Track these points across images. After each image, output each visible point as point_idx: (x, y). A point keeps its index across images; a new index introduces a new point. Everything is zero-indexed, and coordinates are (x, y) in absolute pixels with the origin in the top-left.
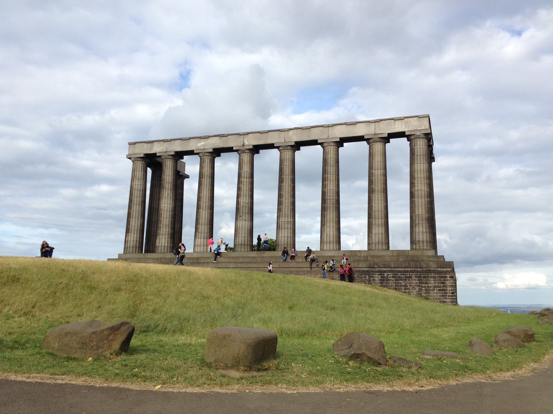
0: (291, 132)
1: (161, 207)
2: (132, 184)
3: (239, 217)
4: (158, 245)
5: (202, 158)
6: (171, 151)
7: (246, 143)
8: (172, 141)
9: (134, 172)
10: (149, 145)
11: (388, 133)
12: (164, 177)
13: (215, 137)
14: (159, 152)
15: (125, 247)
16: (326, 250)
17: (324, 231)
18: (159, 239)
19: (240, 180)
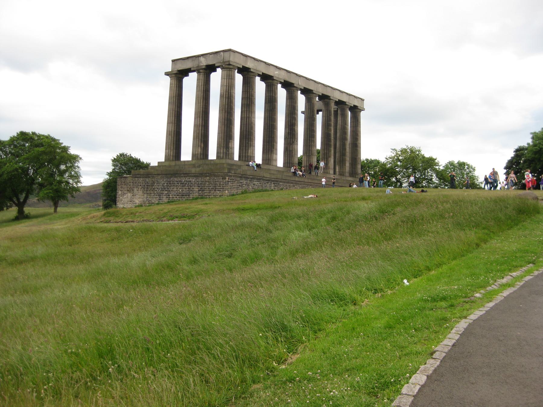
0: (320, 85)
1: (252, 121)
2: (232, 91)
3: (295, 141)
4: (251, 155)
5: (275, 85)
6: (259, 71)
7: (300, 84)
8: (260, 62)
9: (232, 80)
10: (245, 57)
11: (354, 105)
12: (253, 93)
13: (284, 71)
14: (253, 69)
15: (229, 153)
16: (331, 174)
17: (330, 160)
18: (251, 150)
19: (295, 111)
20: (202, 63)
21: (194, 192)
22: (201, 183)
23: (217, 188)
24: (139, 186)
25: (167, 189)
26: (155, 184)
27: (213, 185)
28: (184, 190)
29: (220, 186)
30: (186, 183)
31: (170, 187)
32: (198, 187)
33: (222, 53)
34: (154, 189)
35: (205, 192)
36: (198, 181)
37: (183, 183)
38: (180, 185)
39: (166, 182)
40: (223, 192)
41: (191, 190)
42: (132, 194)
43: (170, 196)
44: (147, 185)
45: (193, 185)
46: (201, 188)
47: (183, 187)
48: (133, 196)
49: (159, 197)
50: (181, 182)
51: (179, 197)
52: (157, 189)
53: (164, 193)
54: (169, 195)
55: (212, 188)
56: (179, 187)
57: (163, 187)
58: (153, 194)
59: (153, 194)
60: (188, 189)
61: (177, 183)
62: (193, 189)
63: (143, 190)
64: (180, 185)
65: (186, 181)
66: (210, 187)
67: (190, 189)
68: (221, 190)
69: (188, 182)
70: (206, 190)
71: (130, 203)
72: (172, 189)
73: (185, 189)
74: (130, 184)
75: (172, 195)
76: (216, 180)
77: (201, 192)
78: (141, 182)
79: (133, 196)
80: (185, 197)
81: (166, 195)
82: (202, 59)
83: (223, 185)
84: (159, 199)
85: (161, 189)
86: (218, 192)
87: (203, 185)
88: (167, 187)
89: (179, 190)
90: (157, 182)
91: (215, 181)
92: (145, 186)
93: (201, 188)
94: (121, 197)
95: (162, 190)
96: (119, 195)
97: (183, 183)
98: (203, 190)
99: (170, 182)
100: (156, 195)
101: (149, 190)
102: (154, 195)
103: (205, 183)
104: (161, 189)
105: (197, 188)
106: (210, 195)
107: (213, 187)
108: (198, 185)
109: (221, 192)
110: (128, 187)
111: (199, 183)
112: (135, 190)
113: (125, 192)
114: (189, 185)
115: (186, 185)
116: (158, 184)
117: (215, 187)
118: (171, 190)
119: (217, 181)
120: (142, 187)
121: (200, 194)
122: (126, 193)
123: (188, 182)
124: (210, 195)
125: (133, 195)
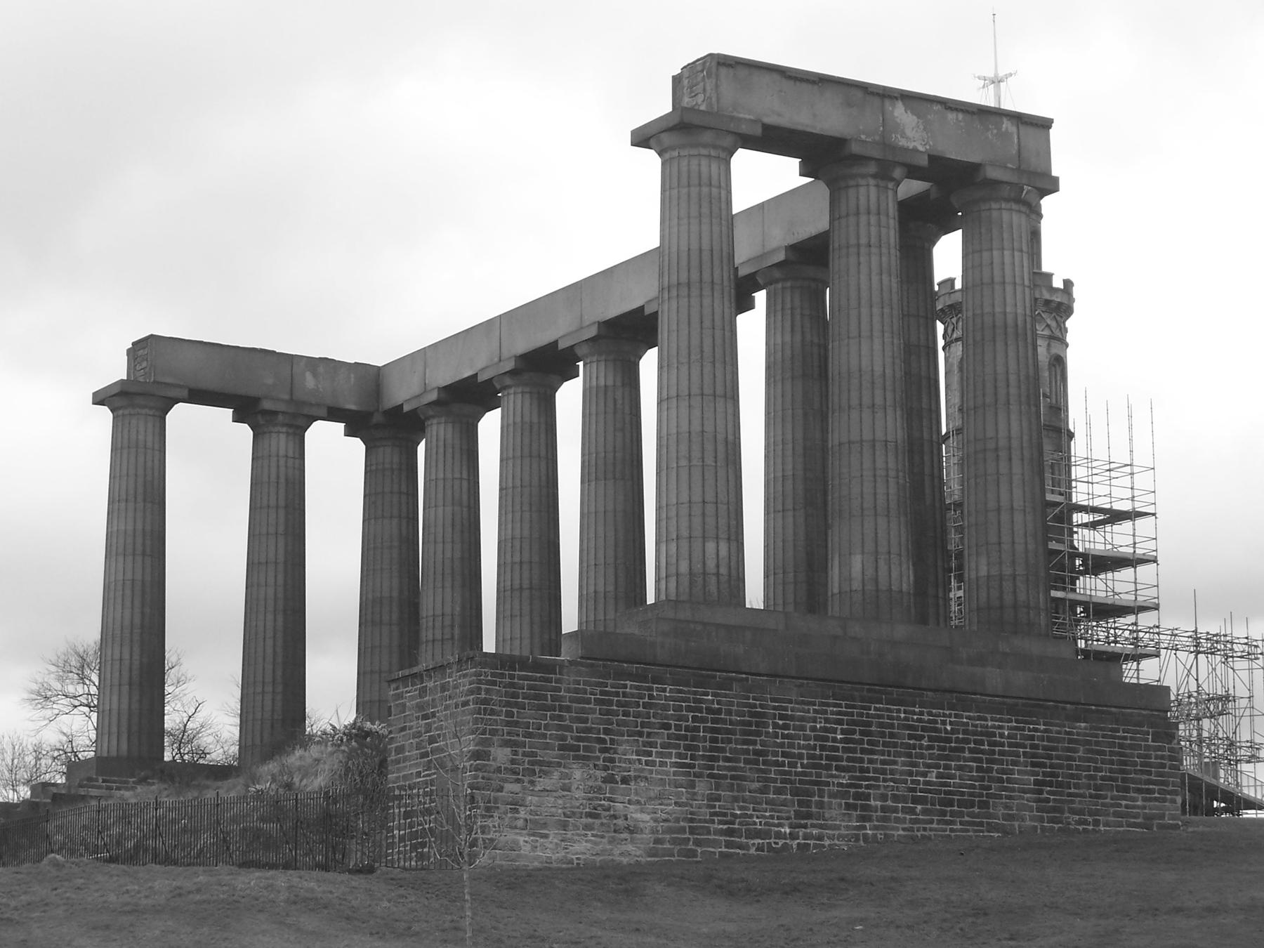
20: (903, 135)
21: (1013, 790)
22: (1045, 748)
23: (1134, 781)
24: (649, 725)
25: (849, 759)
26: (766, 725)
27: (1112, 762)
28: (953, 777)
29: (1150, 773)
30: (967, 741)
31: (863, 751)
32: (1034, 765)
33: (1007, 125)
34: (756, 753)
35: (1070, 795)
36: (1032, 738)
37: (949, 740)
38: (930, 748)
39: (840, 722)
40: (1164, 800)
41: (991, 779)
42: (600, 774)
43: (872, 803)
44: (713, 730)
45: (1002, 753)
46: (1052, 775)
47: (947, 758)
48: (605, 781)
49: (800, 803)
50: (936, 730)
51: (924, 812)
52: (784, 755)
53: (828, 784)
54: (867, 797)
55: (1111, 779)
56: (922, 756)
57: (823, 748)
58: (756, 785)
59: (756, 785)
60: (979, 769)
61: (910, 737)
62: (1004, 772)
63: (679, 756)
64: (930, 748)
65: (965, 732)
66: (1096, 769)
67: (990, 770)
68: (1152, 791)
69: (975, 733)
70: (1077, 786)
71: (588, 827)
72: (884, 762)
73: (959, 768)
74: (583, 711)
75: (884, 798)
76: (1125, 738)
77: (1049, 793)
78: (665, 708)
79: (605, 781)
80: (961, 814)
81: (844, 795)
82: (899, 112)
83: (1163, 766)
84: (798, 815)
85: (810, 757)
86: (1140, 796)
87: (1058, 757)
88: (845, 750)
89: (925, 775)
90: (782, 717)
91: (1121, 746)
92: (697, 729)
93: (1052, 775)
94: (508, 787)
95: (814, 766)
96: (499, 770)
97: (949, 740)
98: (1059, 785)
99: (869, 724)
100: (779, 791)
101: (727, 759)
102: (764, 790)
103: (1069, 750)
104: (810, 757)
105: (1026, 773)
106: (1097, 813)
107: (1111, 771)
108: (1034, 756)
109: (1156, 799)
110: (569, 729)
111: (1033, 747)
112: (627, 751)
113: (551, 755)
114: (982, 752)
115: (962, 749)
116: (786, 727)
117: (1123, 772)
118: (875, 771)
119: (1131, 747)
120: (678, 738)
121: (1048, 800)
122: (549, 764)
123: (975, 733)
124: (1097, 813)
125: (610, 780)
